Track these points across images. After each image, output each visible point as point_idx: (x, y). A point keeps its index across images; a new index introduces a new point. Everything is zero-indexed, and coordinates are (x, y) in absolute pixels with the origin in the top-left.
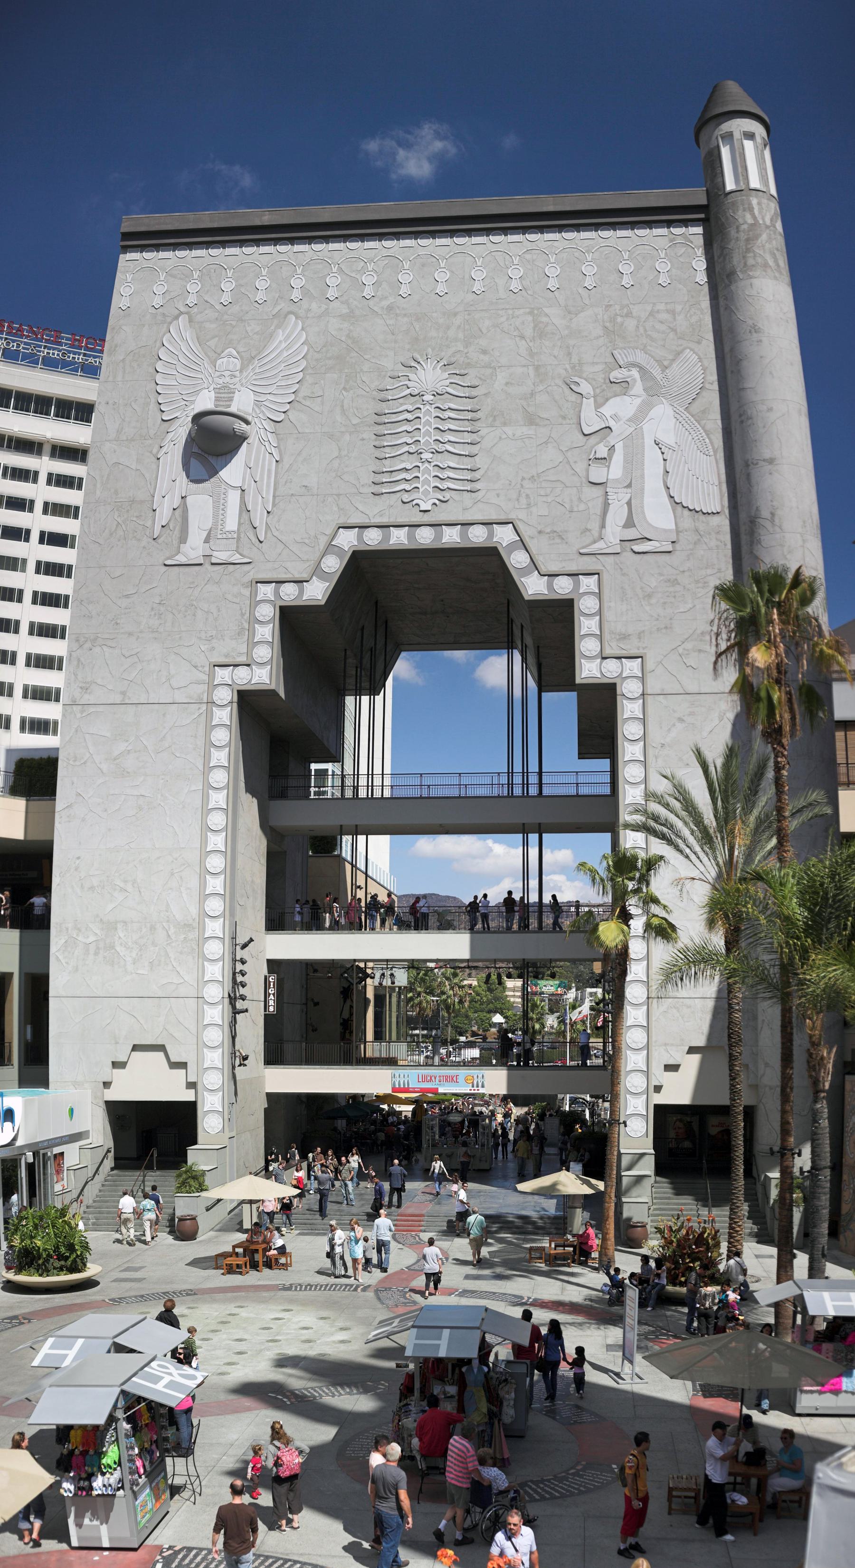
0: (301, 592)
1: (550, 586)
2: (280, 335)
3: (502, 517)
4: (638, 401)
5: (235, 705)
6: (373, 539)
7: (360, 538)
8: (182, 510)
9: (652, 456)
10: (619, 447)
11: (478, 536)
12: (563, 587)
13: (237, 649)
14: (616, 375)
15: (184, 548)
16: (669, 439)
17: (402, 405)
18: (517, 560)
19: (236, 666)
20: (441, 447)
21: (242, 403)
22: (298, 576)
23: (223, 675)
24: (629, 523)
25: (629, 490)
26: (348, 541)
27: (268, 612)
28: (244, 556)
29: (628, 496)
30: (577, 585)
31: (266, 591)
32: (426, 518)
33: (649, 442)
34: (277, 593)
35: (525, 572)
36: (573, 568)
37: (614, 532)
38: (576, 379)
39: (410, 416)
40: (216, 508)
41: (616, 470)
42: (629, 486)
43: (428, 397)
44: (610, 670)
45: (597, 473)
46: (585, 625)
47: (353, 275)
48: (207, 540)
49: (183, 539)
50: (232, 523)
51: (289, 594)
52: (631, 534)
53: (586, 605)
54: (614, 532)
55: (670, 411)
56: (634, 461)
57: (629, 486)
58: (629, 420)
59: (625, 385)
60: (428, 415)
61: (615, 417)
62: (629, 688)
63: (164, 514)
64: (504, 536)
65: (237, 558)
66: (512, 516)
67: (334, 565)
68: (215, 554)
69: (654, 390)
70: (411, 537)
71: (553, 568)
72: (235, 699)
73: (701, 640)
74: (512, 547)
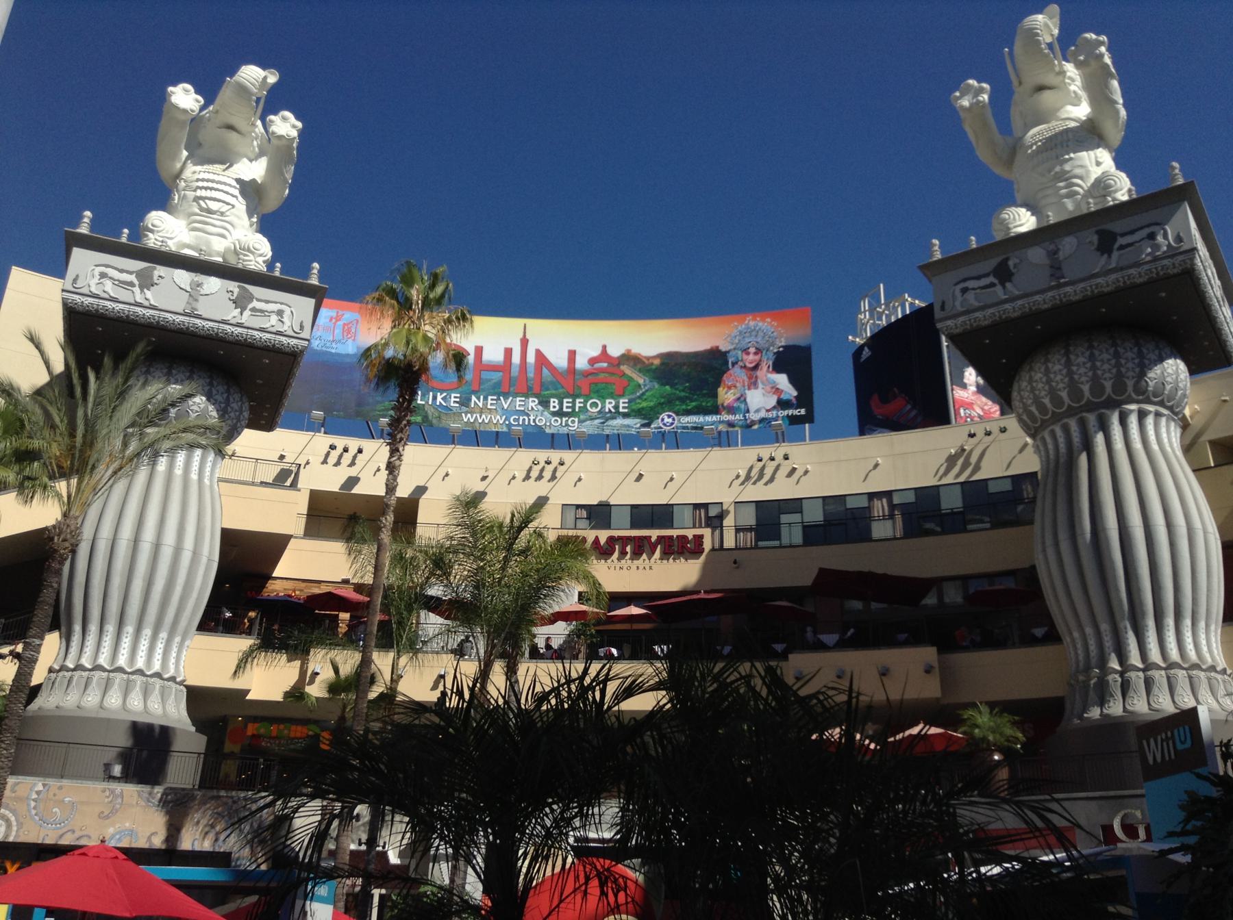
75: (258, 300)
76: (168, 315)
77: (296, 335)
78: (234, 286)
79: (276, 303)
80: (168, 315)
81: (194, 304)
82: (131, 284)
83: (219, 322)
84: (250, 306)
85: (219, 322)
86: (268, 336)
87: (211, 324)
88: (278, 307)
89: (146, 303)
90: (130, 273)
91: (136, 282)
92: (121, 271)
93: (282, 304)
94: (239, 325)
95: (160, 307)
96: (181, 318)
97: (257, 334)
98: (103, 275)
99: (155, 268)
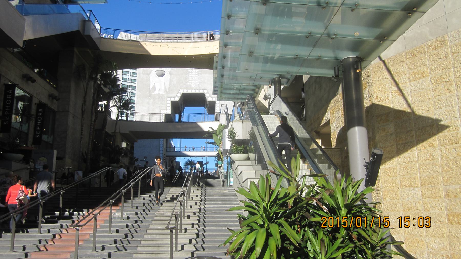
0: (174, 99)
6: (185, 91)
7: (183, 91)
11: (201, 92)
19: (164, 110)
26: (182, 92)
31: (169, 99)
34: (171, 99)
35: (209, 97)
39: (191, 72)
48: (159, 90)
49: (155, 90)
50: (163, 88)
51: (173, 99)
65: (164, 93)
67: (179, 95)
74: (207, 93)
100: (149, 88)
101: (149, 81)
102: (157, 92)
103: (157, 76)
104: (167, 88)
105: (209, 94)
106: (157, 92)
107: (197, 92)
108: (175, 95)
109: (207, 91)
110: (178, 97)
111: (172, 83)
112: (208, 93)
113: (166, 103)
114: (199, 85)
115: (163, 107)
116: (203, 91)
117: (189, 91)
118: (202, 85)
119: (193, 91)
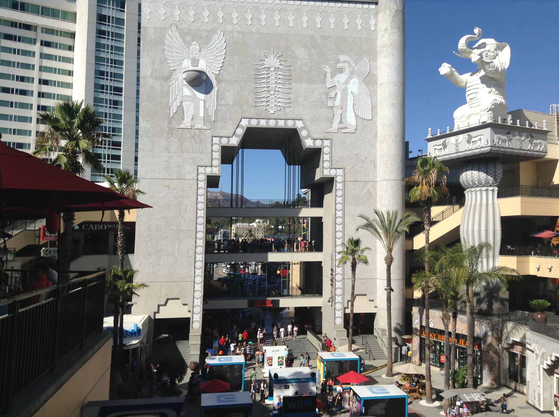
1: (314, 143)
2: (215, 37)
3: (299, 118)
4: (347, 76)
5: (206, 181)
6: (254, 123)
7: (249, 122)
8: (181, 106)
9: (350, 97)
10: (339, 94)
11: (290, 124)
12: (318, 144)
13: (207, 162)
14: (339, 65)
15: (184, 122)
16: (356, 91)
17: (263, 71)
18: (303, 134)
20: (277, 89)
21: (202, 66)
22: (227, 135)
23: (201, 170)
24: (341, 122)
25: (342, 110)
26: (245, 123)
27: (217, 148)
28: (208, 127)
29: (341, 112)
30: (323, 143)
31: (216, 140)
32: (273, 116)
33: (349, 91)
35: (307, 137)
36: (321, 136)
37: (336, 125)
38: (325, 66)
40: (195, 108)
41: (338, 103)
42: (342, 108)
43: (272, 69)
44: (332, 173)
45: (330, 103)
46: (325, 157)
47: (243, 13)
48: (192, 119)
50: (202, 114)
51: (224, 142)
52: (341, 126)
53: (326, 150)
54: (336, 125)
55: (357, 81)
56: (344, 99)
57: (342, 108)
58: (343, 83)
59: (341, 71)
60: (273, 76)
61: (339, 82)
62: (339, 179)
63: (174, 109)
64: (299, 125)
65: (204, 127)
66: (302, 117)
67: (240, 132)
68: (196, 125)
69: (352, 73)
70: (267, 123)
71: (316, 136)
72: (206, 179)
73: (362, 164)
75: (474, 137)
76: (452, 155)
77: (486, 146)
78: (466, 135)
79: (478, 136)
80: (452, 155)
81: (457, 148)
82: (441, 149)
83: (464, 151)
84: (471, 141)
85: (464, 151)
86: (478, 150)
87: (463, 153)
88: (478, 138)
89: (446, 154)
90: (440, 145)
91: (442, 148)
92: (439, 145)
93: (480, 135)
94: (470, 150)
95: (450, 153)
96: (455, 155)
97: (475, 151)
98: (435, 149)
99: (446, 140)
100: (170, 113)
101: (168, 95)
102: (187, 122)
103: (185, 83)
104: (211, 112)
105: (307, 130)
106: (187, 122)
107: (281, 124)
108: (229, 132)
109: (304, 123)
110: (238, 136)
111: (223, 102)
112: (305, 128)
113: (210, 149)
114: (284, 107)
115: (202, 159)
116: (295, 124)
117: (263, 123)
118: (291, 109)
119: (272, 124)
